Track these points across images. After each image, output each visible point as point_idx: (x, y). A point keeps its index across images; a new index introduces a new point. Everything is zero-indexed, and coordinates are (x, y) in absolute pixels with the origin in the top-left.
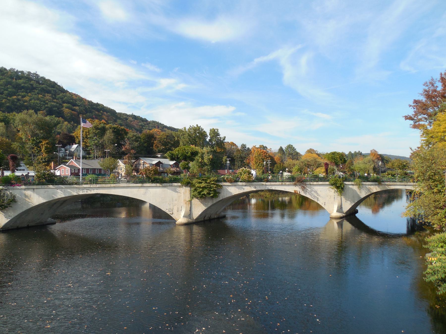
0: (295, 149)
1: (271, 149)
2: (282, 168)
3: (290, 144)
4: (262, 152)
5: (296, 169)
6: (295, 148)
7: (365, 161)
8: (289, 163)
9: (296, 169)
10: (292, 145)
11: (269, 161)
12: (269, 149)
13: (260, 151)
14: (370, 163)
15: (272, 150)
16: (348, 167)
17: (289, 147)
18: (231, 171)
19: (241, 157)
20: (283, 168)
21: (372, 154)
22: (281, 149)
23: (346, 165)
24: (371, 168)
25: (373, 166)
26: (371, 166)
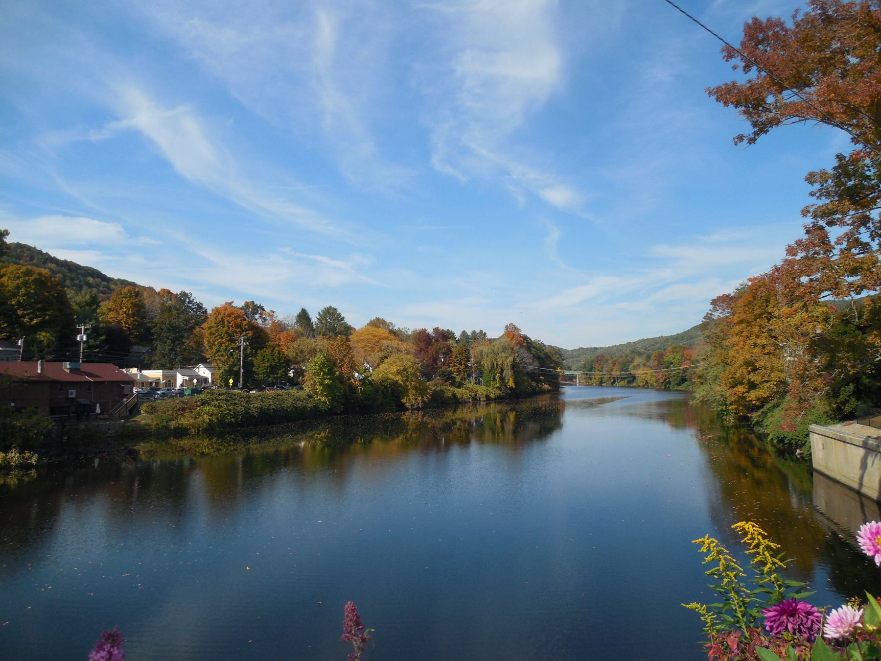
0: (343, 318)
1: (274, 312)
2: (276, 359)
3: (330, 307)
4: (229, 316)
5: (316, 363)
6: (342, 316)
7: (495, 349)
8: (299, 345)
9: (316, 363)
10: (335, 309)
11: (242, 339)
12: (269, 314)
13: (222, 313)
14: (505, 352)
15: (275, 315)
16: (458, 360)
17: (330, 314)
18: (68, 366)
19: (173, 328)
20: (279, 359)
21: (509, 334)
22: (304, 316)
23: (454, 357)
24: (507, 365)
25: (511, 359)
26: (508, 361)
